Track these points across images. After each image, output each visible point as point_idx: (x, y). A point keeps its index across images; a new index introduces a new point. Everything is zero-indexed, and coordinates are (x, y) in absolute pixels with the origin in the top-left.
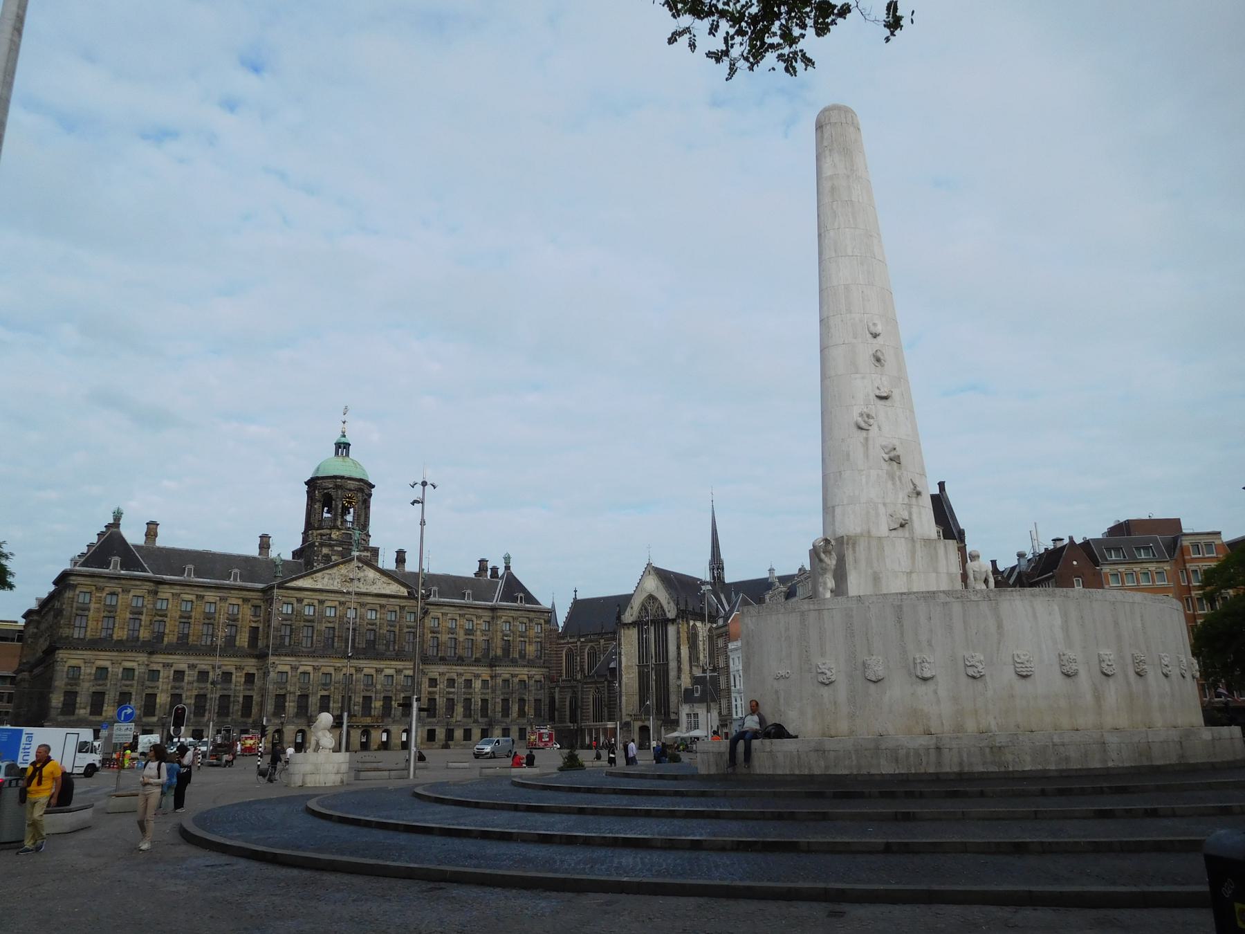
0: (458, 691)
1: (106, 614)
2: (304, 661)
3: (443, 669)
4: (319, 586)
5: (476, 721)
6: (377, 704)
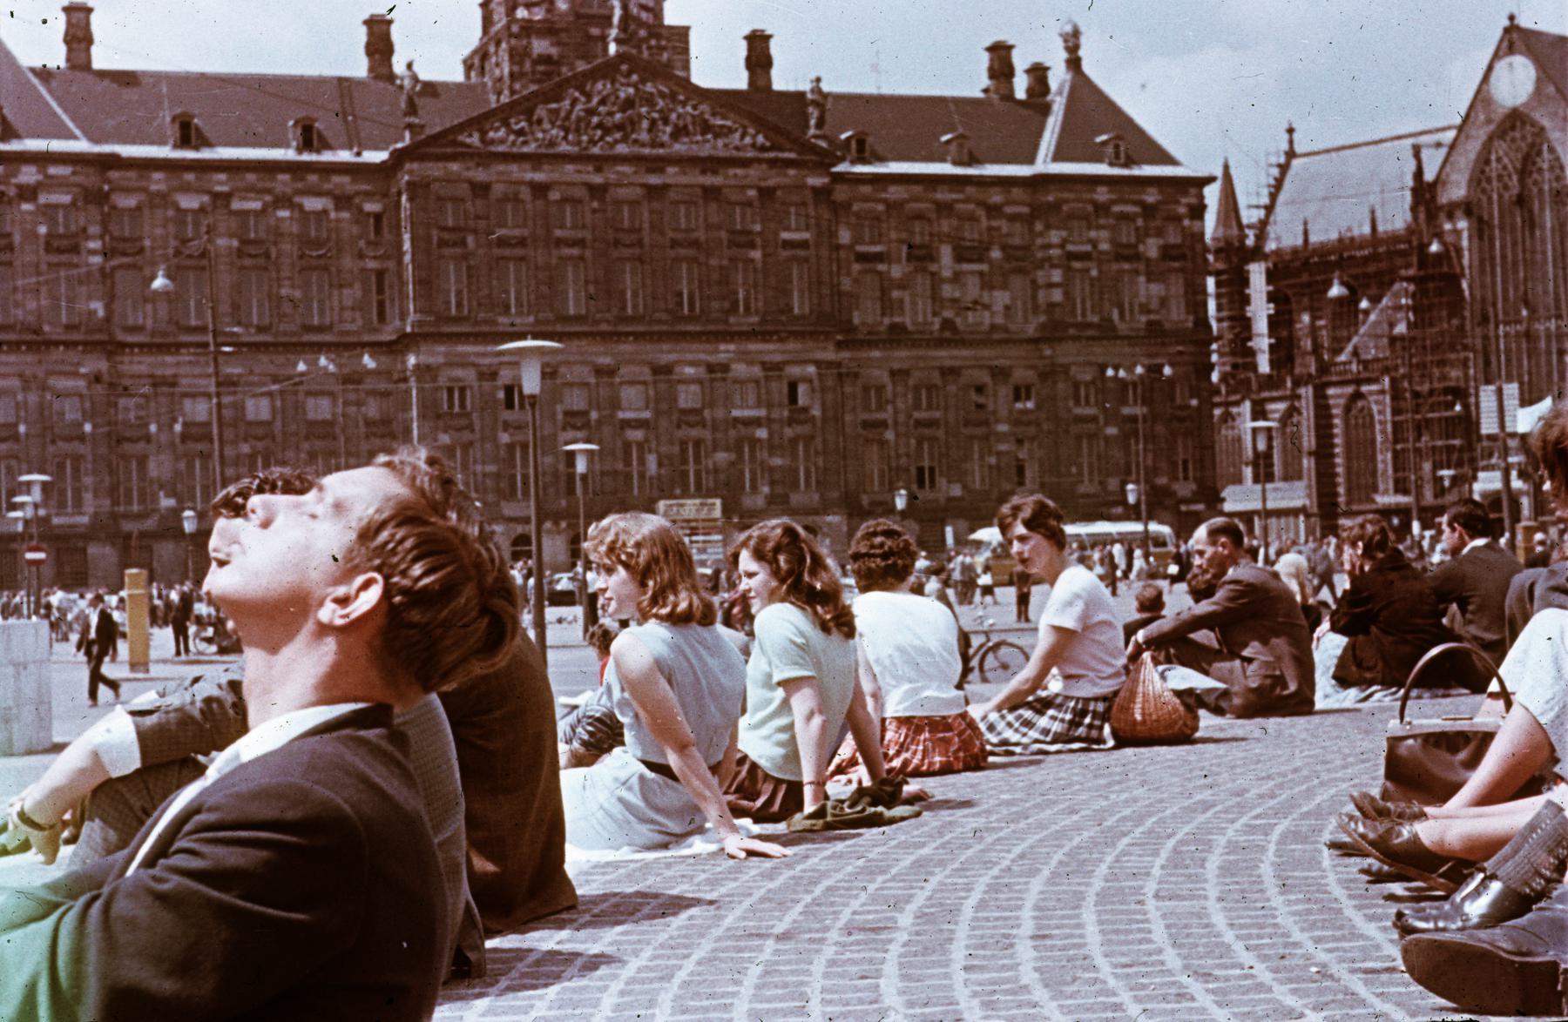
3: (901, 356)
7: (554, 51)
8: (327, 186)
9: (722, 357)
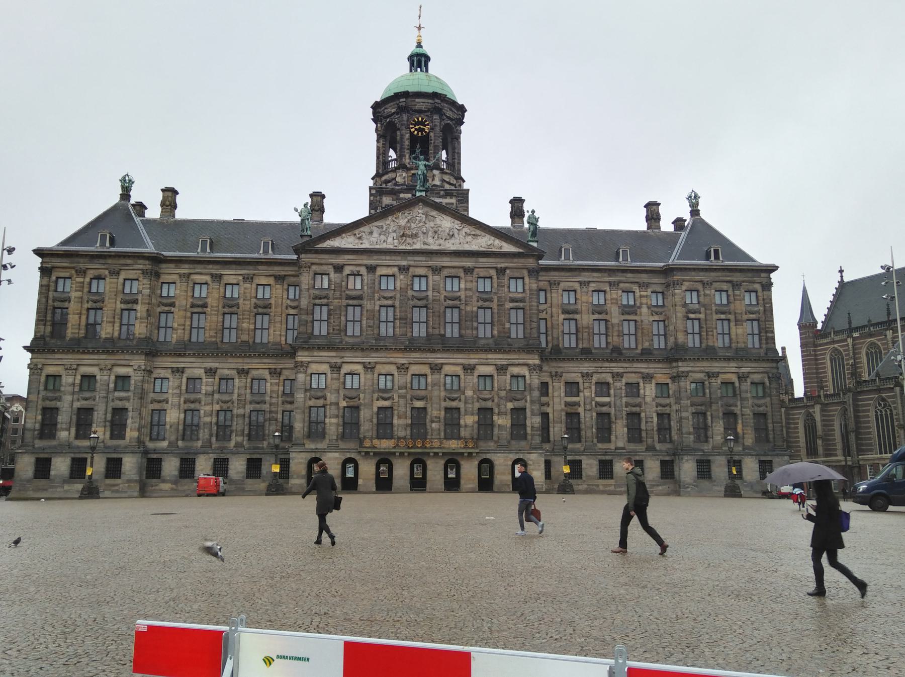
0: (617, 402)
1: (90, 305)
2: (349, 356)
3: (587, 367)
4: (366, 245)
5: (651, 448)
6: (469, 420)
7: (395, 203)
8: (271, 272)
9: (473, 362)
